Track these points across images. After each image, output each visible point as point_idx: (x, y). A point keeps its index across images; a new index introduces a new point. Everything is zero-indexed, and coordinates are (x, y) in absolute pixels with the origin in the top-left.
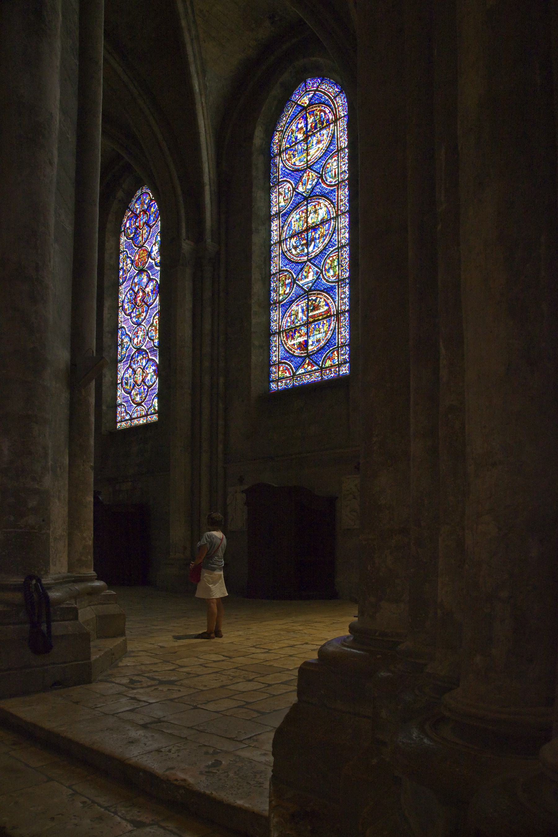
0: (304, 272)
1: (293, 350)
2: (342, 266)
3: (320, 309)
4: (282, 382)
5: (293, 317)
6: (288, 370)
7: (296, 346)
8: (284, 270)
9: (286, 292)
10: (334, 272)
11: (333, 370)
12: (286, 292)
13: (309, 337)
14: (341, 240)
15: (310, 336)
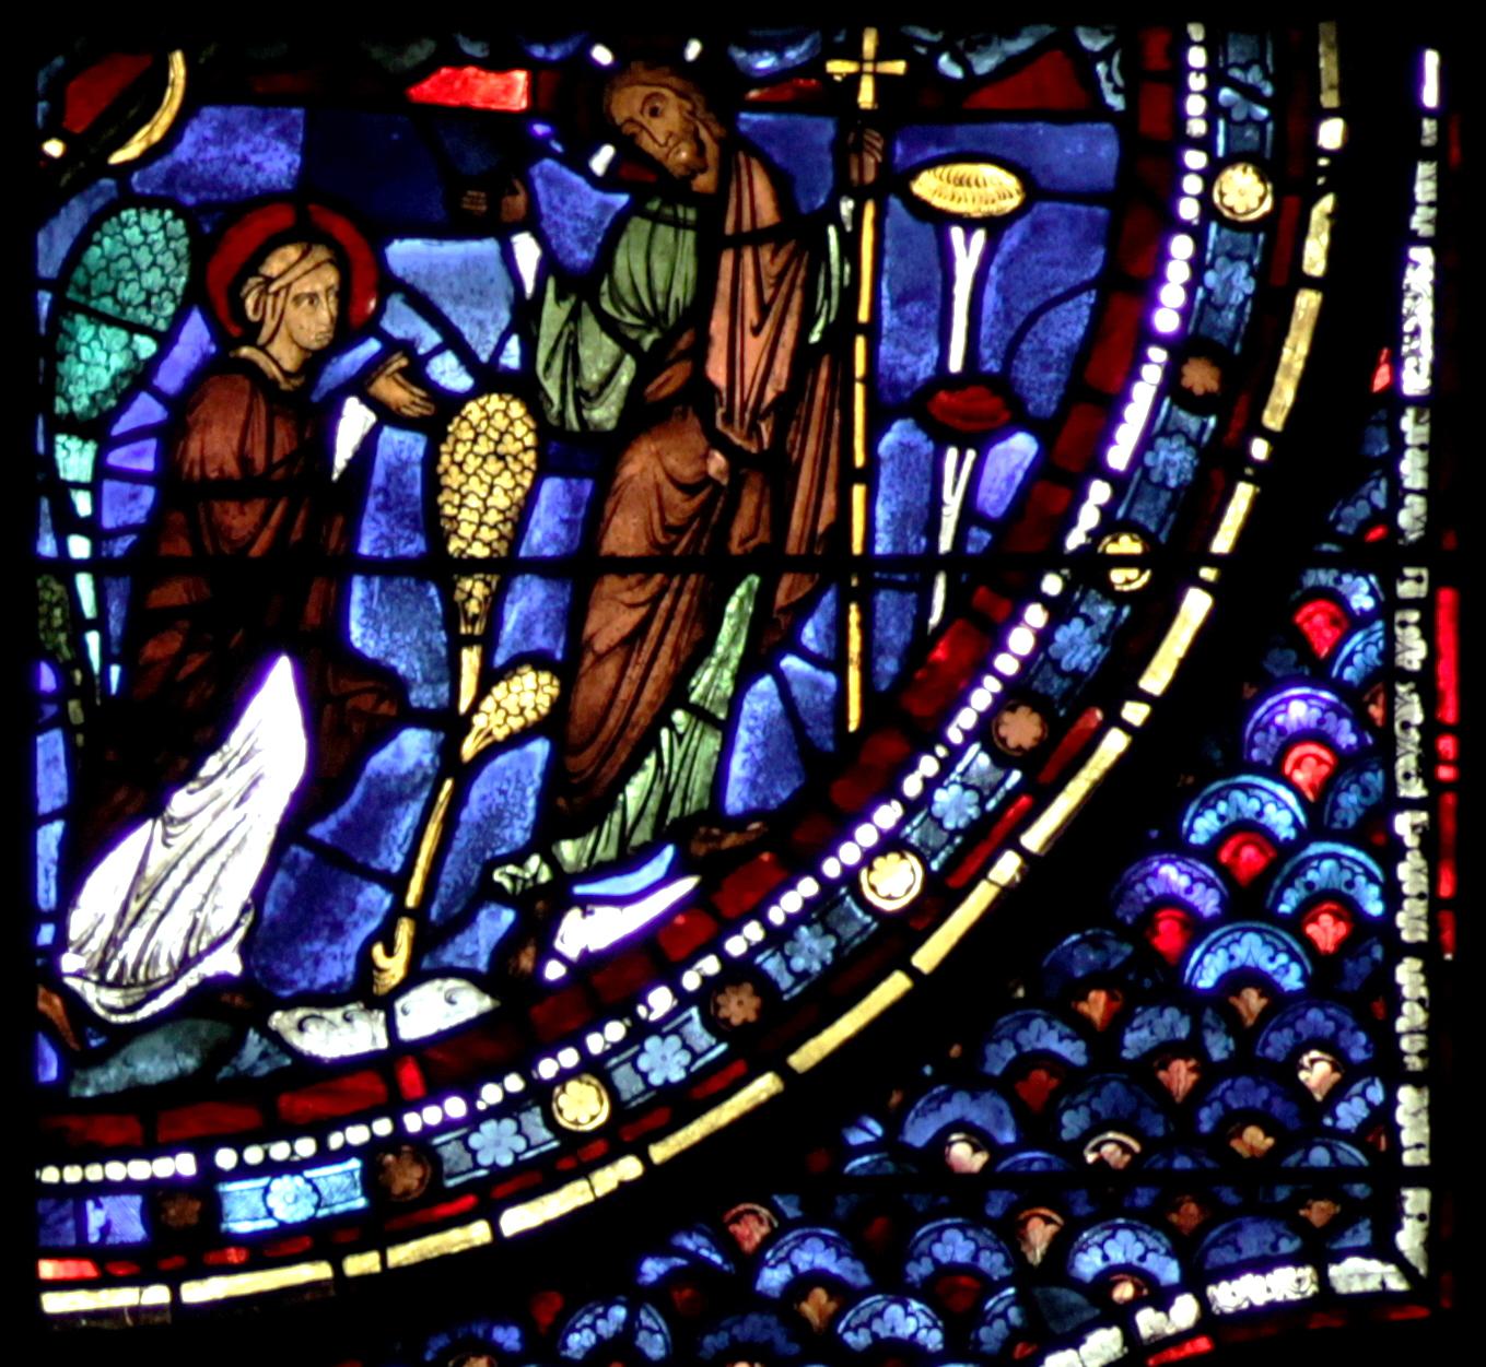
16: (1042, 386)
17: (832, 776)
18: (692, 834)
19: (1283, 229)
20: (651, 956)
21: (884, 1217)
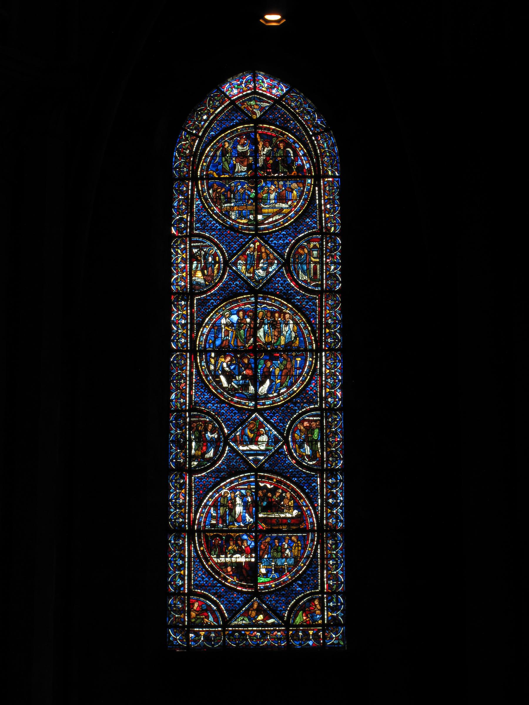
0: (248, 431)
1: (223, 574)
2: (329, 446)
3: (282, 512)
4: (197, 634)
5: (221, 511)
6: (213, 612)
7: (229, 569)
8: (201, 411)
9: (207, 456)
10: (314, 451)
11: (311, 632)
12: (207, 456)
13: (259, 559)
14: (326, 398)
15: (262, 558)
16: (302, 367)
17: (292, 385)
18: (286, 387)
19: (312, 361)
20: (285, 392)
21: (295, 404)
